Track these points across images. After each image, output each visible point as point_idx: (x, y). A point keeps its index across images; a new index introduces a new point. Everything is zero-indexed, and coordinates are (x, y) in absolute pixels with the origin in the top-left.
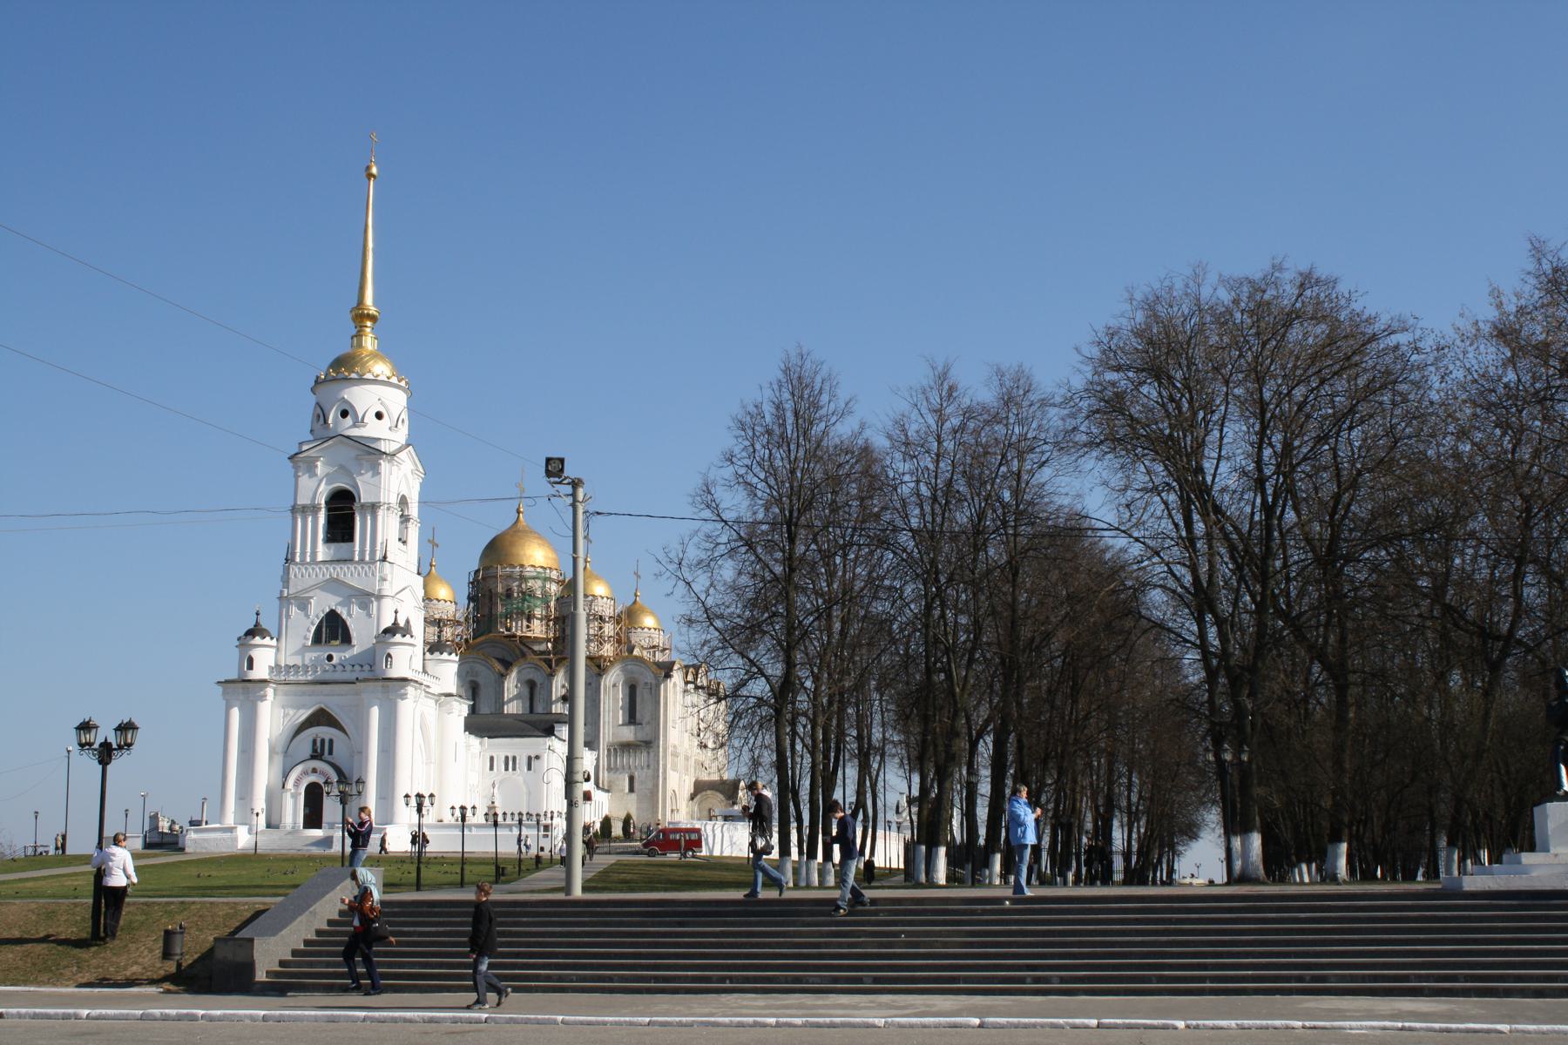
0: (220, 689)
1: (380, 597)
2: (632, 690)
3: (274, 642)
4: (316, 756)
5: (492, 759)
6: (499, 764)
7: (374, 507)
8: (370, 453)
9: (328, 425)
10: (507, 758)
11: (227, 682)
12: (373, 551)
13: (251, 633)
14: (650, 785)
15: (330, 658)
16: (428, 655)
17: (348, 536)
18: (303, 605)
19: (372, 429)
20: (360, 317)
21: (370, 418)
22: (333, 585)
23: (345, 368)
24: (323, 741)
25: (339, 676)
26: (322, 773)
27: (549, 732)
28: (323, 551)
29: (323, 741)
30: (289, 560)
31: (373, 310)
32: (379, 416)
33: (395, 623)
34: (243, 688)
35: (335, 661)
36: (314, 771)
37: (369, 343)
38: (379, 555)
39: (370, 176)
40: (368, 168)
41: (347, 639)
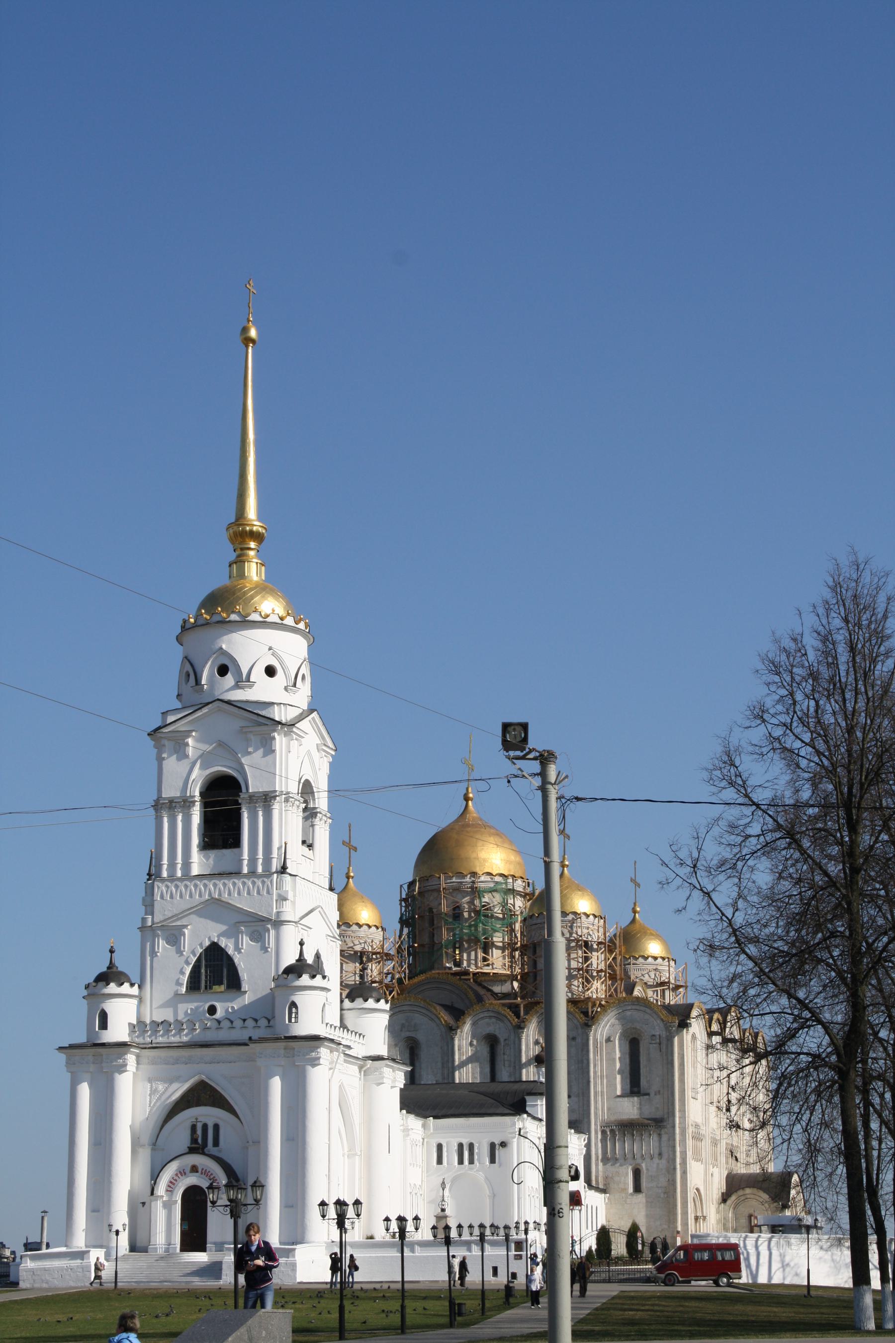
0: (62, 1057)
1: (278, 923)
2: (633, 1046)
3: (135, 990)
4: (197, 1147)
5: (440, 1147)
7: (267, 799)
8: (259, 724)
9: (201, 688)
10: (461, 1146)
11: (72, 1047)
12: (268, 860)
13: (104, 978)
14: (663, 1181)
15: (212, 1010)
16: (347, 1004)
17: (234, 842)
18: (174, 938)
19: (262, 690)
20: (240, 536)
22: (215, 908)
23: (222, 607)
24: (205, 1127)
25: (224, 1035)
26: (206, 1173)
27: (519, 1108)
28: (198, 863)
29: (205, 1127)
31: (257, 526)
32: (270, 671)
33: (301, 959)
34: (94, 1055)
35: (219, 1014)
36: (194, 1169)
37: (254, 571)
38: (275, 865)
39: (248, 340)
40: (245, 330)
41: (234, 983)
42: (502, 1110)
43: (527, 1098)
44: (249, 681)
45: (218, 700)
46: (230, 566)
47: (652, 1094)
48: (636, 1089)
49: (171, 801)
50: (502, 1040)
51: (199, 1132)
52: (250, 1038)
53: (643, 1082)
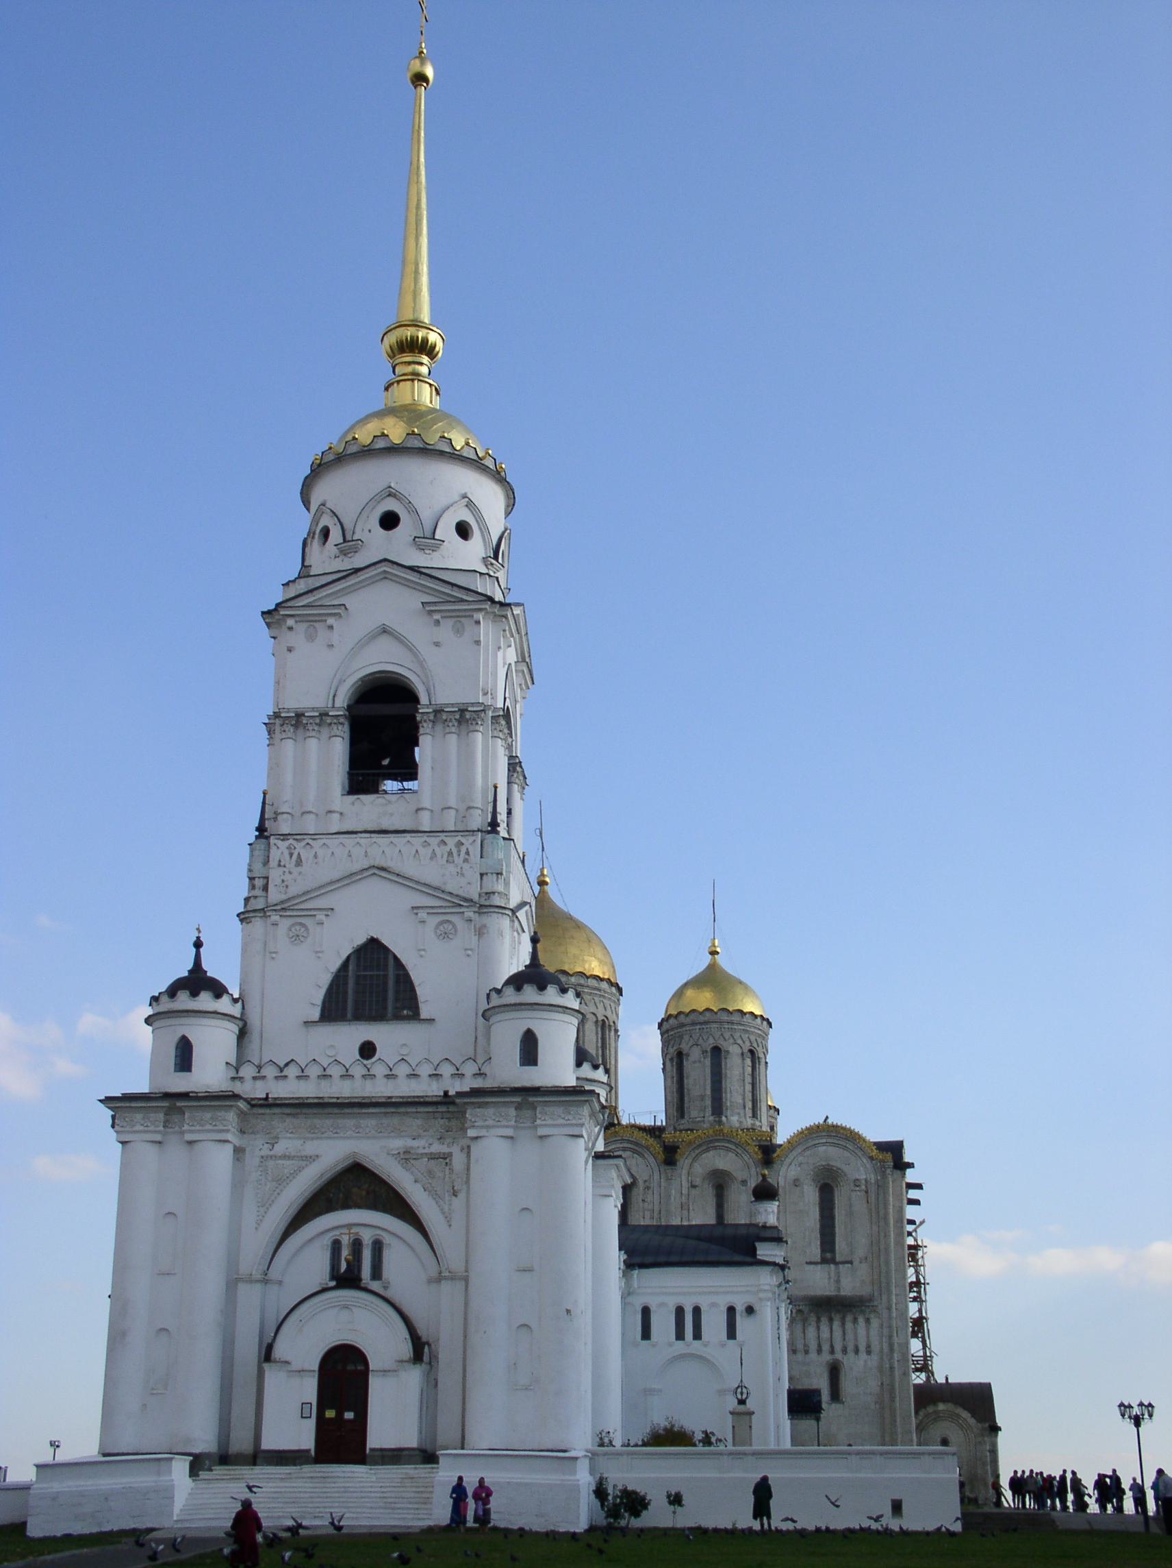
4: (346, 1278)
5: (646, 1312)
6: (663, 1324)
10: (680, 1311)
11: (128, 1097)
15: (367, 1050)
21: (446, 531)
24: (357, 1245)
29: (357, 1245)
30: (261, 829)
38: (478, 820)
39: (420, 78)
42: (737, 1258)
43: (757, 1244)
45: (385, 560)
46: (387, 389)
47: (856, 1263)
48: (828, 1255)
49: (299, 715)
50: (641, 1182)
51: (345, 1252)
52: (446, 1093)
53: (841, 1245)
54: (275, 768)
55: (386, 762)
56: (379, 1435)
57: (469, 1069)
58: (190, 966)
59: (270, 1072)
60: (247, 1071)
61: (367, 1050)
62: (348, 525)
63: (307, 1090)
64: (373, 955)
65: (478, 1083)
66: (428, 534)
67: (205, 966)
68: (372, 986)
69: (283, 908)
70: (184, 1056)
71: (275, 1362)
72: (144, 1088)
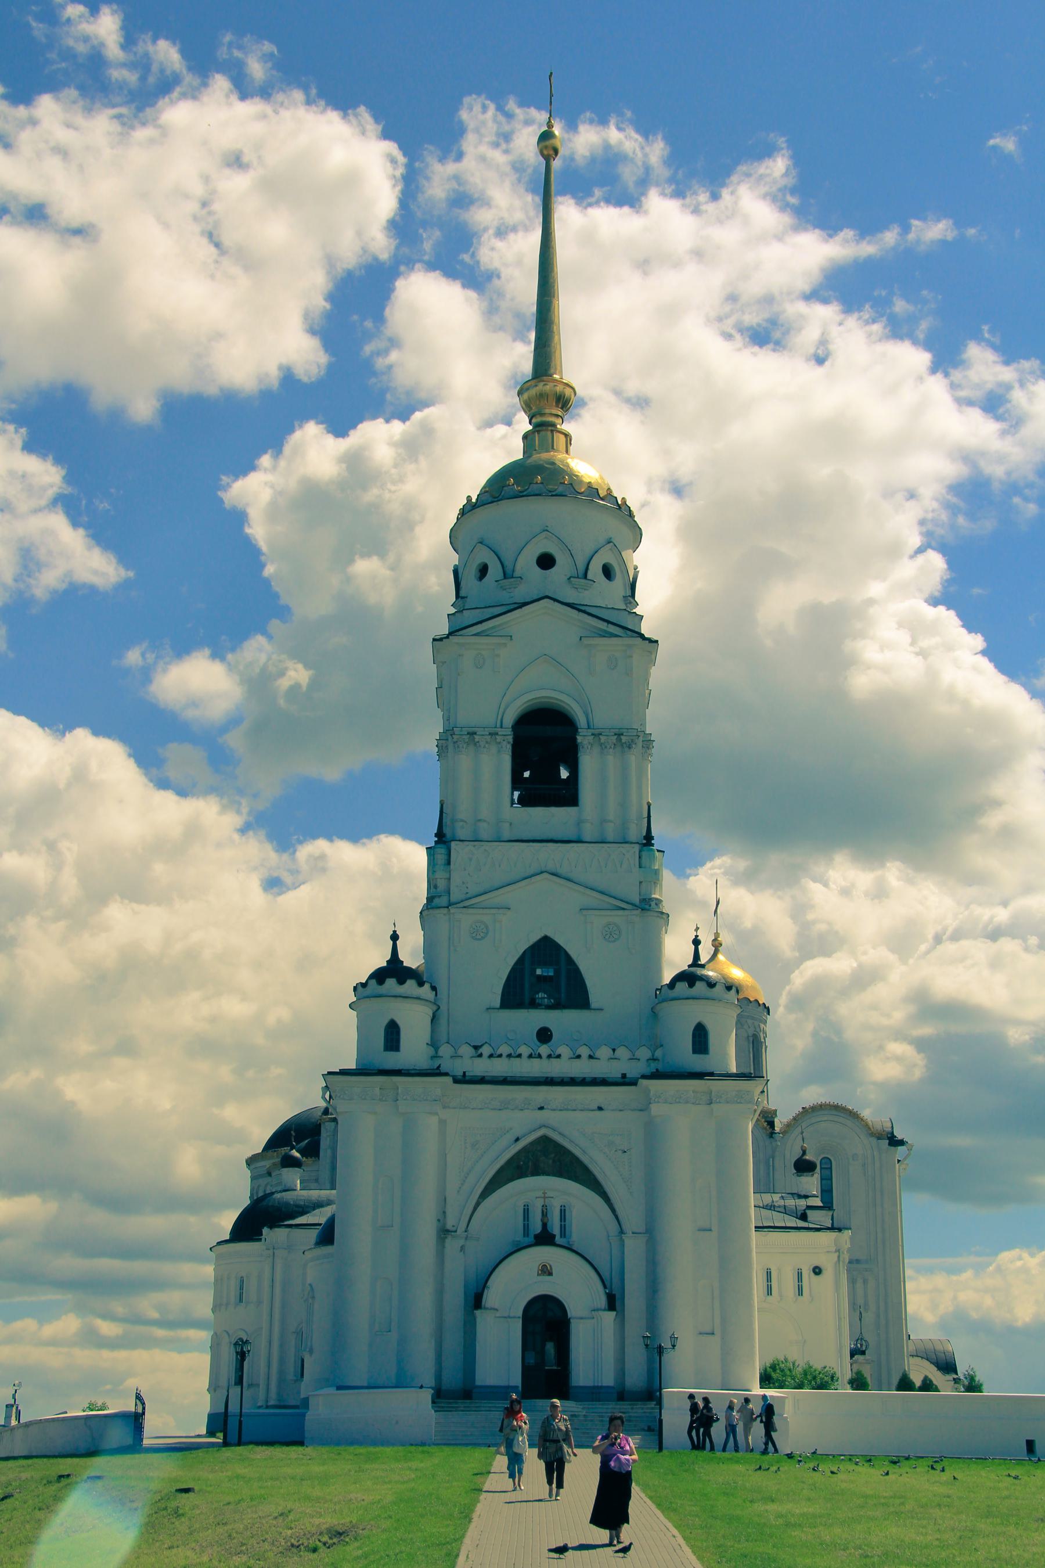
4: (545, 1238)
11: (343, 1072)
17: (567, 795)
21: (595, 571)
30: (440, 835)
36: (546, 1271)
38: (636, 833)
44: (585, 576)
49: (472, 734)
52: (624, 1076)
54: (448, 780)
55: (527, 774)
56: (581, 1374)
57: (644, 1053)
58: (389, 957)
59: (466, 1051)
60: (445, 1050)
61: (544, 1035)
62: (509, 565)
63: (499, 1068)
64: (545, 950)
65: (653, 1067)
66: (581, 575)
67: (401, 957)
68: (546, 977)
69: (464, 903)
70: (392, 1035)
71: (486, 1309)
72: (352, 1065)
